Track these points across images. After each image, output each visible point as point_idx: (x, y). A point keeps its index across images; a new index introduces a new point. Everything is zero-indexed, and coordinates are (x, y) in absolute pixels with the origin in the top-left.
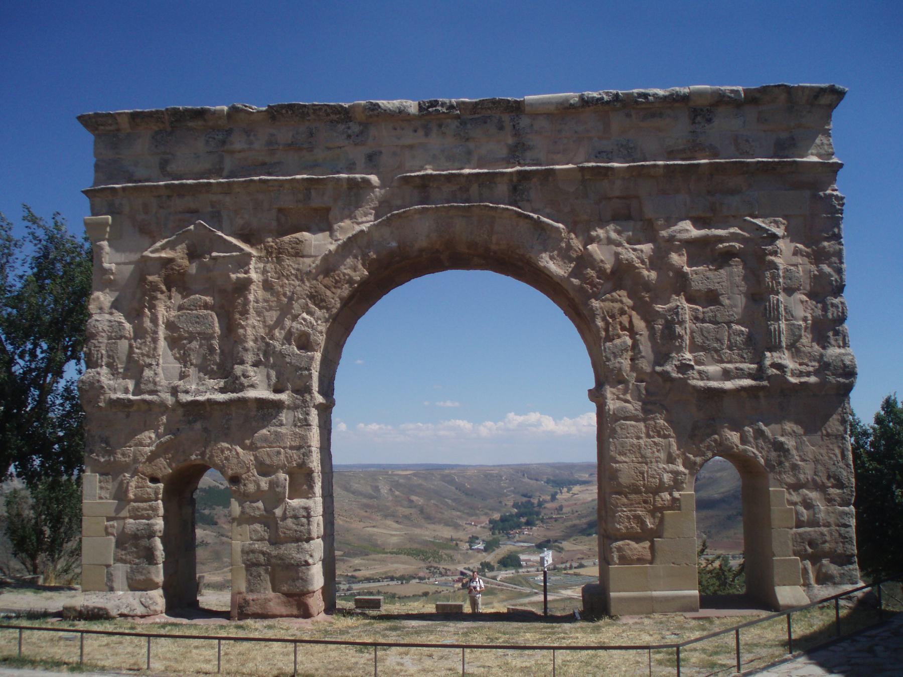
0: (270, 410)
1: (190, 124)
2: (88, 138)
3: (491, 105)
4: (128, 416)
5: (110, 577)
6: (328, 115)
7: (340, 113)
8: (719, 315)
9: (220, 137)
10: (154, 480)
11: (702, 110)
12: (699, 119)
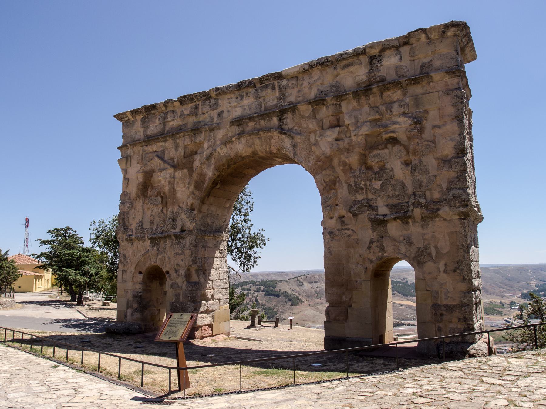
0: (180, 240)
1: (153, 112)
2: (120, 124)
3: (267, 78)
4: (132, 245)
5: (126, 316)
6: (201, 97)
7: (205, 96)
8: (385, 175)
9: (163, 116)
10: (140, 273)
11: (375, 56)
12: (374, 61)
